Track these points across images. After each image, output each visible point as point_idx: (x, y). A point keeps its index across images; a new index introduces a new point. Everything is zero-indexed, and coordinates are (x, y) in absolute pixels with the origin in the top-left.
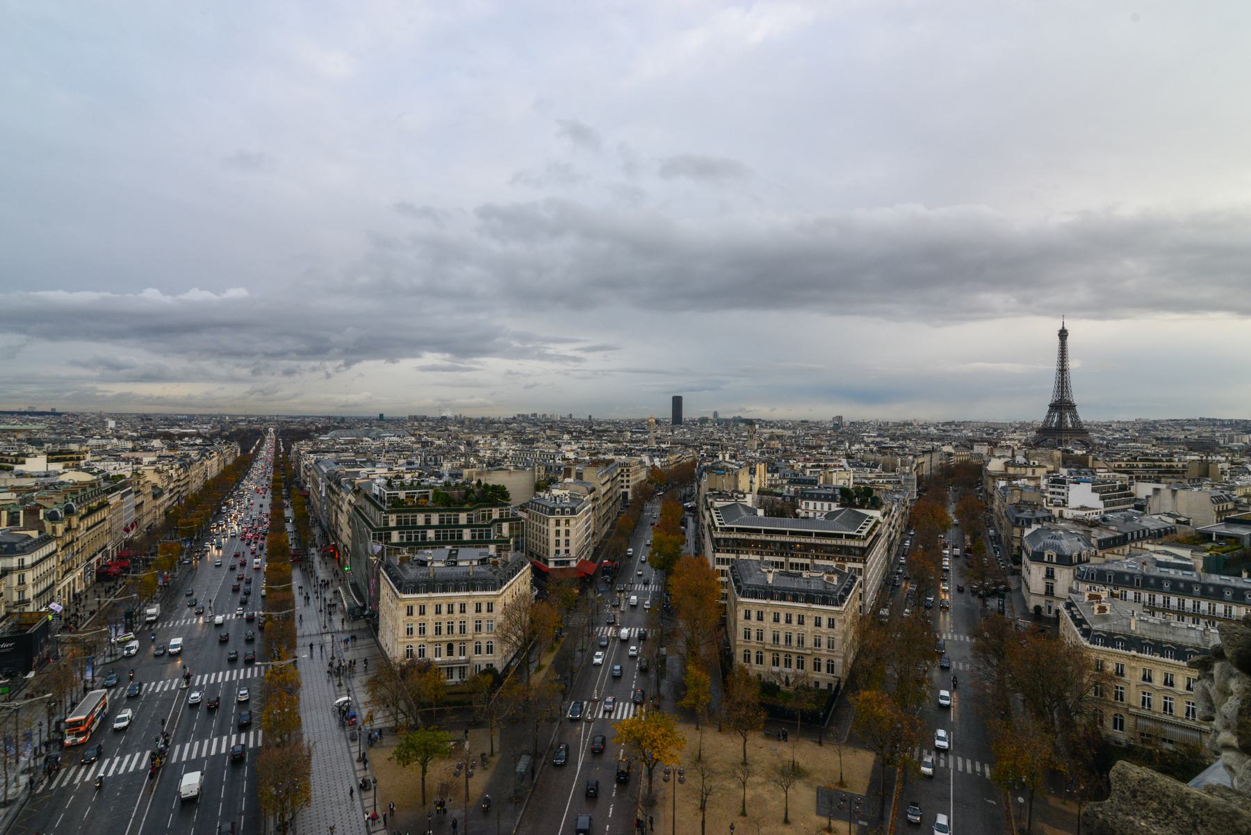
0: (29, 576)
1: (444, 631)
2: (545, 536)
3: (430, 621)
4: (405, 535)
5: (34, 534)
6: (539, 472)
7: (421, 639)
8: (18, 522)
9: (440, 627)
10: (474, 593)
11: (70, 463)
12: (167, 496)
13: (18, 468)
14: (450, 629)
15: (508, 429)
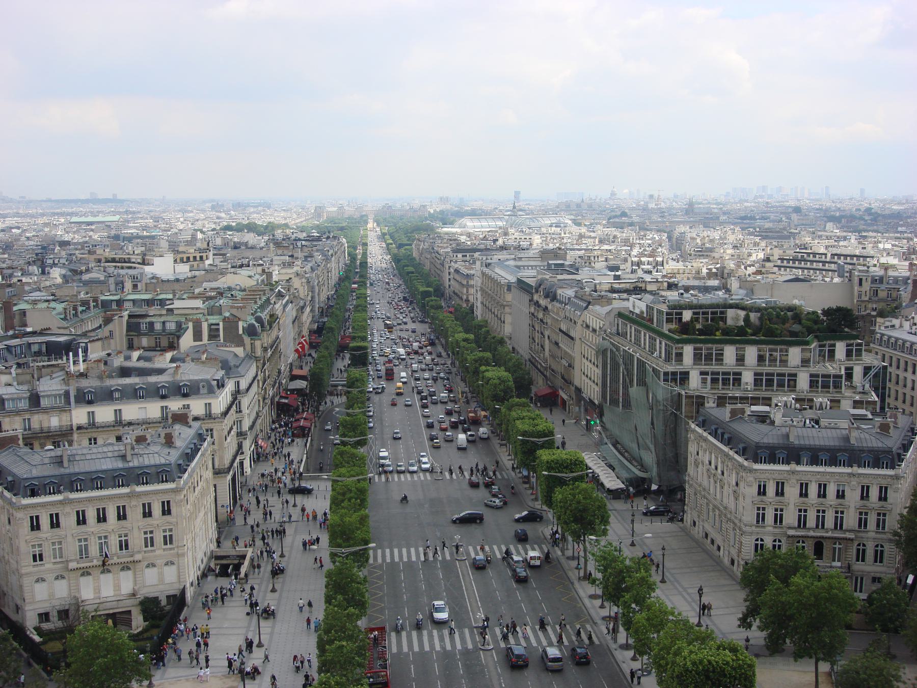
0: (245, 401)
1: (811, 522)
2: (908, 390)
3: (792, 506)
4: (709, 378)
5: (240, 351)
6: (860, 284)
7: (777, 531)
8: (219, 336)
9: (805, 516)
10: (862, 471)
11: (195, 263)
12: (308, 309)
13: (147, 269)
14: (820, 522)
15: (724, 213)
